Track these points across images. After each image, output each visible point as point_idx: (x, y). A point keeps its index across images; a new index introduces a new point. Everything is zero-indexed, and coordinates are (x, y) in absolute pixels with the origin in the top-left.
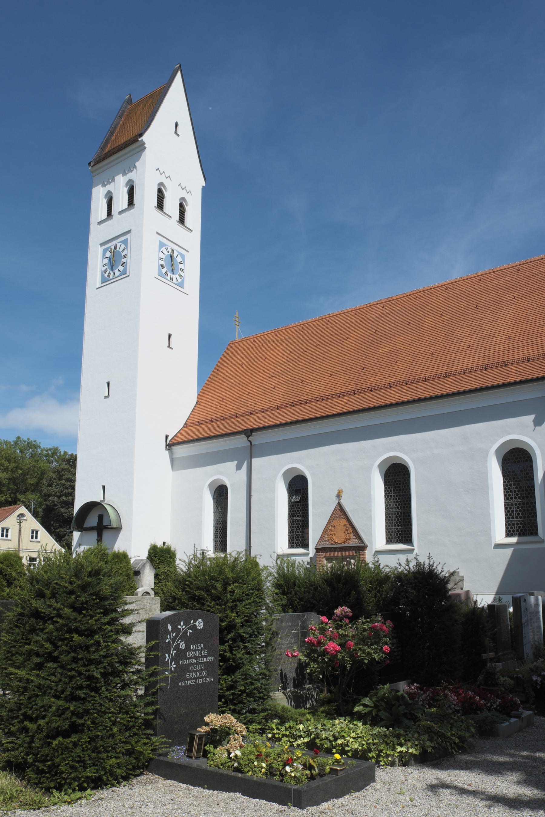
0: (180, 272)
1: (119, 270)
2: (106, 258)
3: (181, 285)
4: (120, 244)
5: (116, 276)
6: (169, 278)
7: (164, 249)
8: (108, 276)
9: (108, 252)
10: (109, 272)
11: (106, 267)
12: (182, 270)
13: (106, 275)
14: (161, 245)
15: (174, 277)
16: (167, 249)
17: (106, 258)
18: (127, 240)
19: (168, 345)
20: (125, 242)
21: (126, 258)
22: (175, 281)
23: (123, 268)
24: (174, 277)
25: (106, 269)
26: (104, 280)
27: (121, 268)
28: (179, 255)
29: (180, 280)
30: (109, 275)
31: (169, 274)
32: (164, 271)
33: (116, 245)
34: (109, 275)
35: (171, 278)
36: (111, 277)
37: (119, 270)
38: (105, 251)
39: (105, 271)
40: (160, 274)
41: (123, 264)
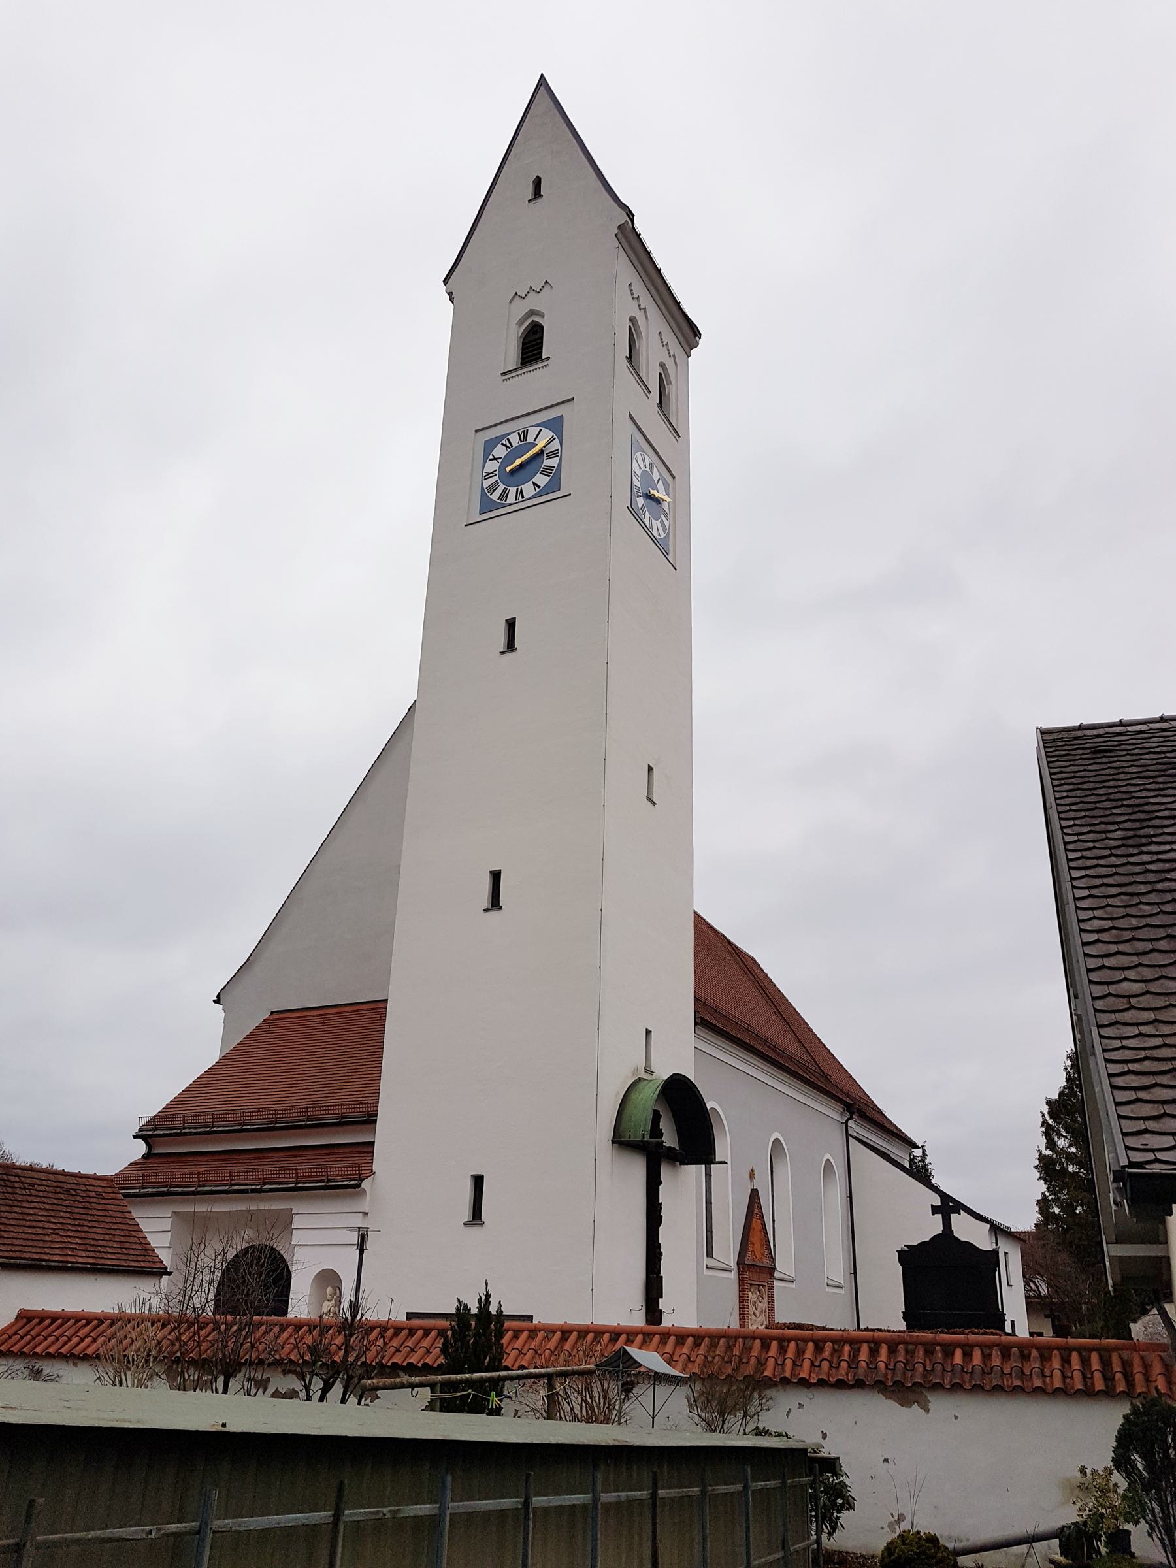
1: (534, 484)
8: (501, 498)
10: (505, 490)
13: (495, 497)
20: (556, 425)
21: (558, 458)
23: (549, 478)
26: (487, 506)
27: (542, 480)
30: (504, 496)
33: (526, 433)
34: (504, 496)
36: (511, 499)
37: (534, 484)
38: (490, 445)
39: (493, 488)
41: (547, 471)
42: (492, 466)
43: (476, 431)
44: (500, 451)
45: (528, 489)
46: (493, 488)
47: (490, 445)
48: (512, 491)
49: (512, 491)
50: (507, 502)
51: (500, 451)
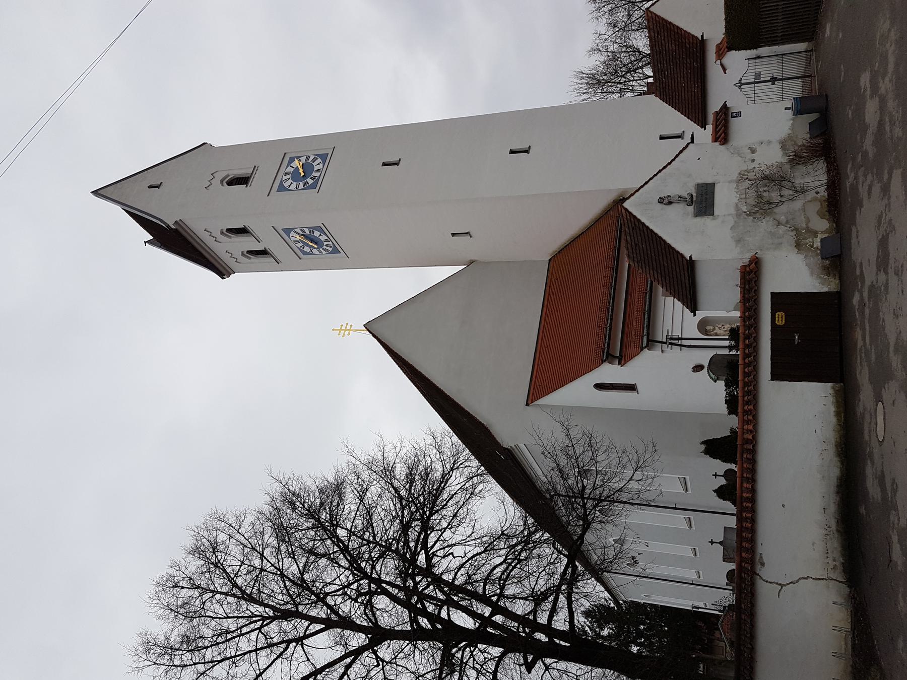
0: (309, 161)
2: (311, 251)
3: (324, 157)
4: (291, 237)
5: (327, 238)
6: (318, 174)
7: (286, 185)
9: (304, 250)
11: (321, 249)
12: (307, 159)
13: (330, 249)
14: (282, 188)
15: (316, 168)
16: (286, 181)
17: (311, 251)
18: (284, 230)
19: (395, 166)
22: (321, 166)
23: (315, 231)
24: (316, 168)
25: (323, 249)
26: (335, 251)
28: (291, 165)
29: (319, 160)
31: (314, 174)
32: (310, 181)
33: (294, 241)
35: (318, 171)
36: (330, 243)
37: (320, 235)
38: (305, 253)
39: (327, 250)
40: (313, 186)
42: (315, 251)
43: (300, 259)
44: (307, 249)
45: (323, 238)
46: (327, 250)
47: (305, 253)
48: (325, 243)
49: (325, 243)
50: (290, 188)
51: (307, 249)
